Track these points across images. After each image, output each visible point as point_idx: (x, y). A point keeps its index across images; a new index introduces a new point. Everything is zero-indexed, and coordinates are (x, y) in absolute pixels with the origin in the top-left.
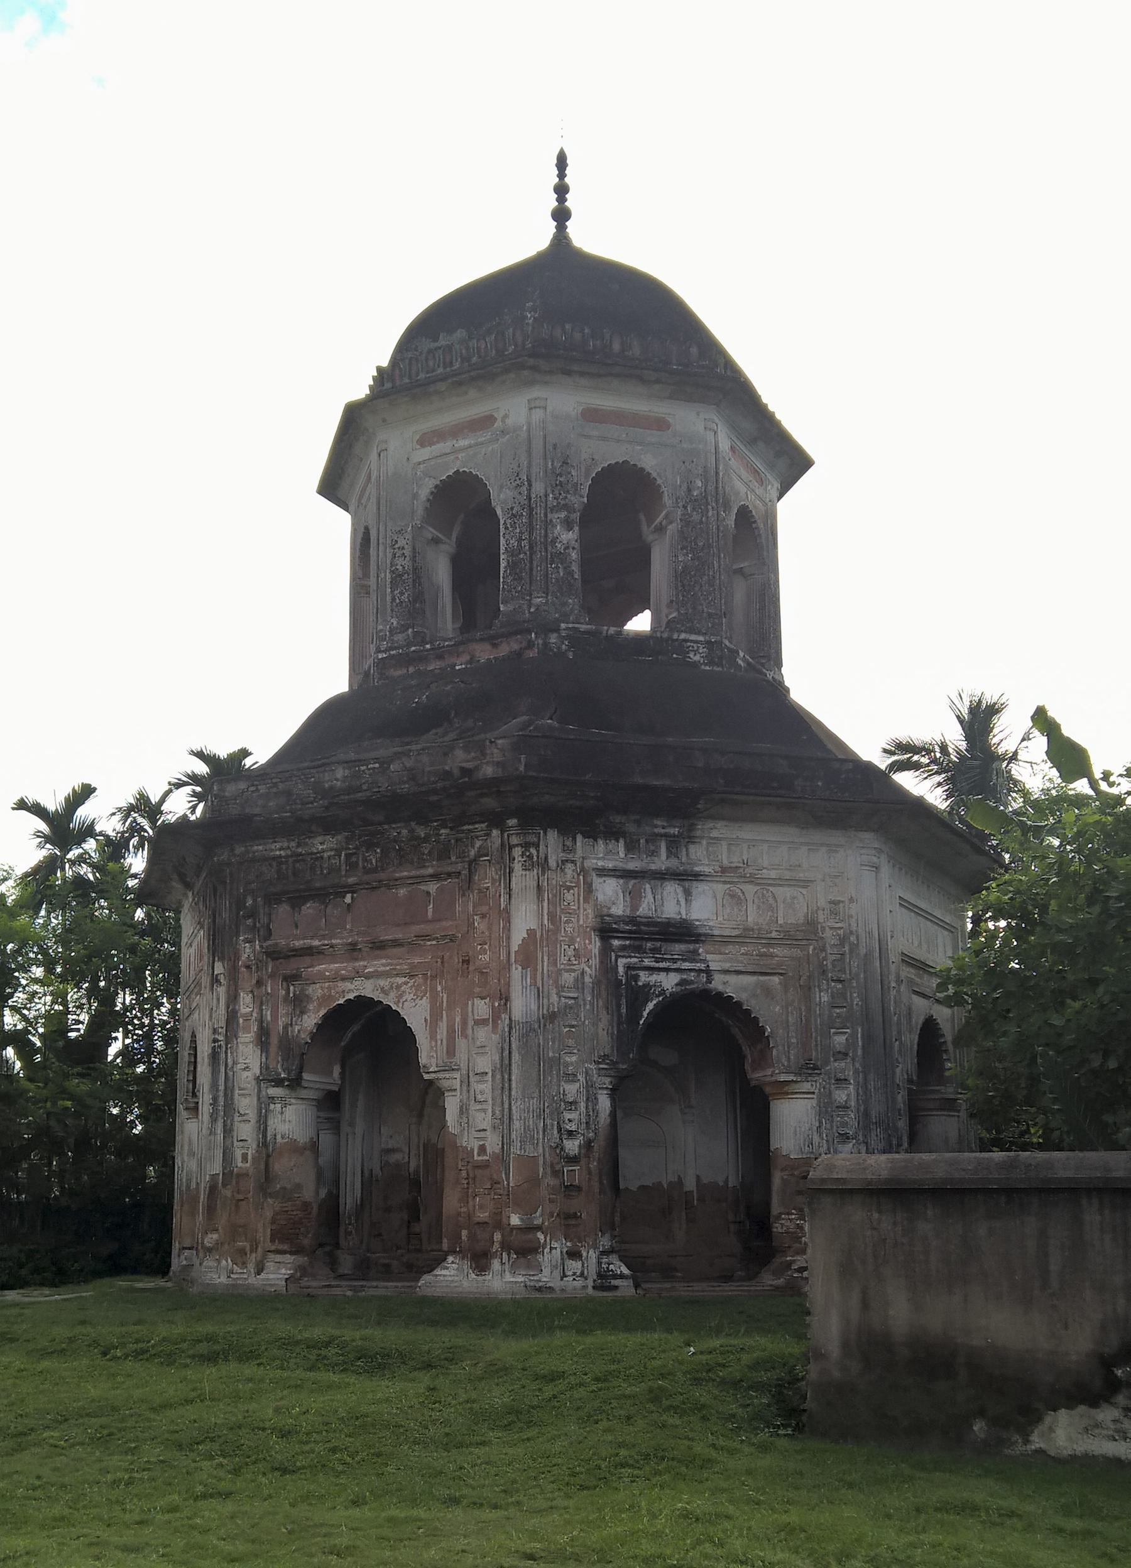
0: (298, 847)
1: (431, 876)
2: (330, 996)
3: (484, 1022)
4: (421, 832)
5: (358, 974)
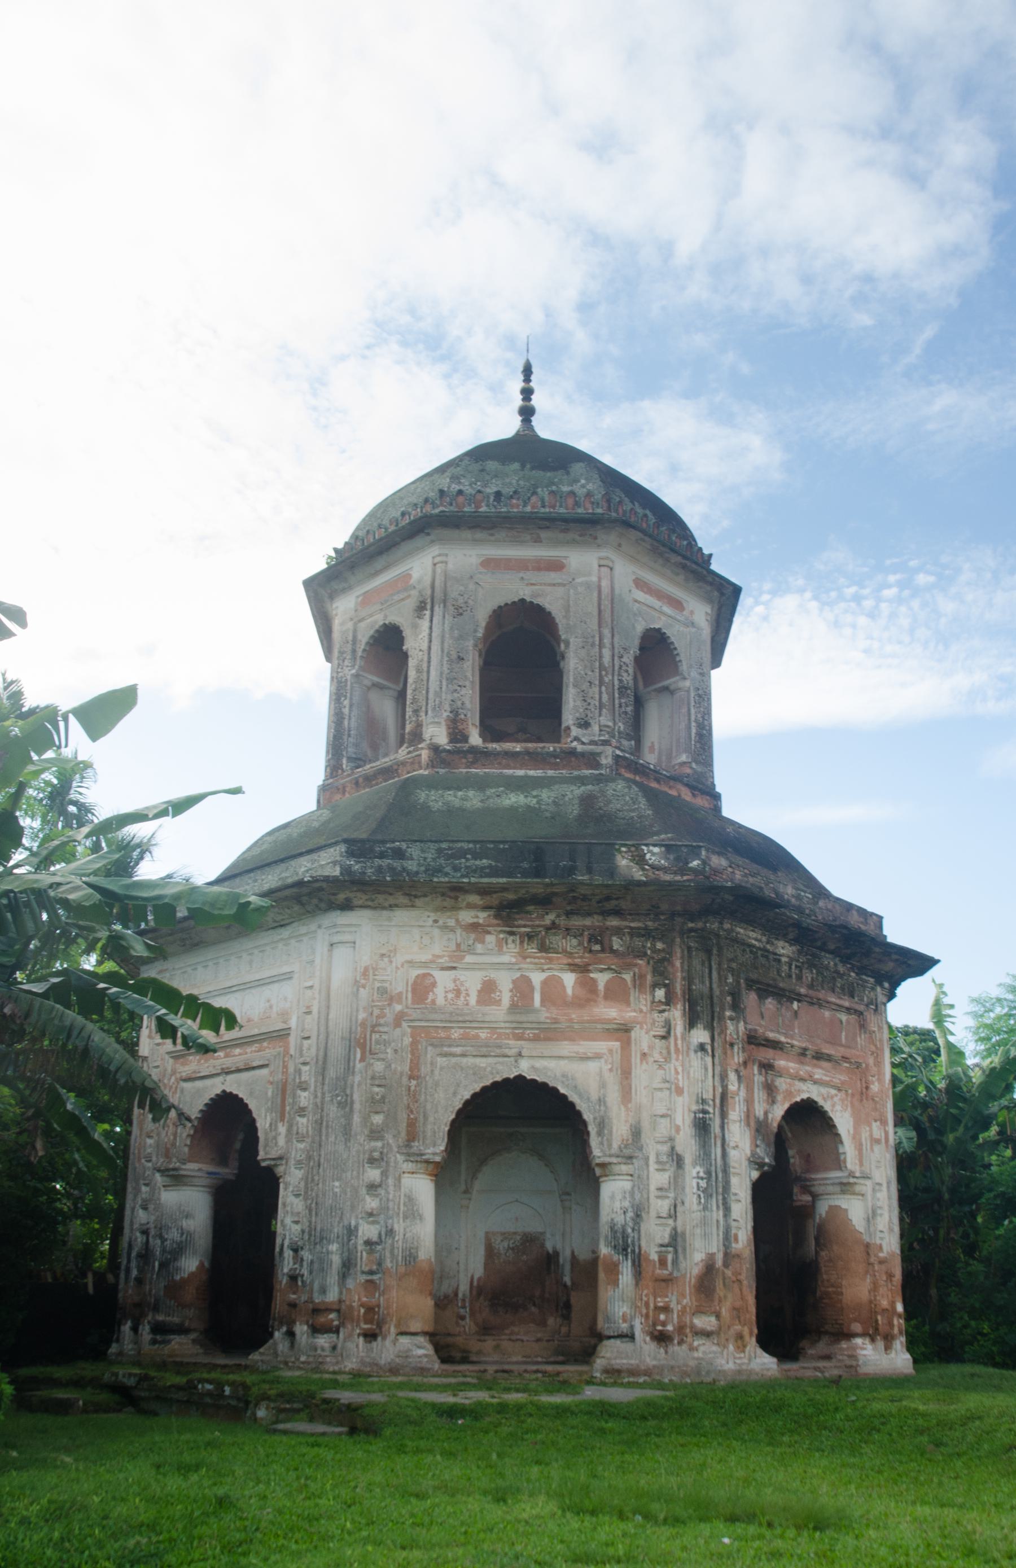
0: (768, 943)
1: (848, 1009)
2: (791, 1092)
3: (878, 1141)
4: (841, 969)
5: (810, 1079)
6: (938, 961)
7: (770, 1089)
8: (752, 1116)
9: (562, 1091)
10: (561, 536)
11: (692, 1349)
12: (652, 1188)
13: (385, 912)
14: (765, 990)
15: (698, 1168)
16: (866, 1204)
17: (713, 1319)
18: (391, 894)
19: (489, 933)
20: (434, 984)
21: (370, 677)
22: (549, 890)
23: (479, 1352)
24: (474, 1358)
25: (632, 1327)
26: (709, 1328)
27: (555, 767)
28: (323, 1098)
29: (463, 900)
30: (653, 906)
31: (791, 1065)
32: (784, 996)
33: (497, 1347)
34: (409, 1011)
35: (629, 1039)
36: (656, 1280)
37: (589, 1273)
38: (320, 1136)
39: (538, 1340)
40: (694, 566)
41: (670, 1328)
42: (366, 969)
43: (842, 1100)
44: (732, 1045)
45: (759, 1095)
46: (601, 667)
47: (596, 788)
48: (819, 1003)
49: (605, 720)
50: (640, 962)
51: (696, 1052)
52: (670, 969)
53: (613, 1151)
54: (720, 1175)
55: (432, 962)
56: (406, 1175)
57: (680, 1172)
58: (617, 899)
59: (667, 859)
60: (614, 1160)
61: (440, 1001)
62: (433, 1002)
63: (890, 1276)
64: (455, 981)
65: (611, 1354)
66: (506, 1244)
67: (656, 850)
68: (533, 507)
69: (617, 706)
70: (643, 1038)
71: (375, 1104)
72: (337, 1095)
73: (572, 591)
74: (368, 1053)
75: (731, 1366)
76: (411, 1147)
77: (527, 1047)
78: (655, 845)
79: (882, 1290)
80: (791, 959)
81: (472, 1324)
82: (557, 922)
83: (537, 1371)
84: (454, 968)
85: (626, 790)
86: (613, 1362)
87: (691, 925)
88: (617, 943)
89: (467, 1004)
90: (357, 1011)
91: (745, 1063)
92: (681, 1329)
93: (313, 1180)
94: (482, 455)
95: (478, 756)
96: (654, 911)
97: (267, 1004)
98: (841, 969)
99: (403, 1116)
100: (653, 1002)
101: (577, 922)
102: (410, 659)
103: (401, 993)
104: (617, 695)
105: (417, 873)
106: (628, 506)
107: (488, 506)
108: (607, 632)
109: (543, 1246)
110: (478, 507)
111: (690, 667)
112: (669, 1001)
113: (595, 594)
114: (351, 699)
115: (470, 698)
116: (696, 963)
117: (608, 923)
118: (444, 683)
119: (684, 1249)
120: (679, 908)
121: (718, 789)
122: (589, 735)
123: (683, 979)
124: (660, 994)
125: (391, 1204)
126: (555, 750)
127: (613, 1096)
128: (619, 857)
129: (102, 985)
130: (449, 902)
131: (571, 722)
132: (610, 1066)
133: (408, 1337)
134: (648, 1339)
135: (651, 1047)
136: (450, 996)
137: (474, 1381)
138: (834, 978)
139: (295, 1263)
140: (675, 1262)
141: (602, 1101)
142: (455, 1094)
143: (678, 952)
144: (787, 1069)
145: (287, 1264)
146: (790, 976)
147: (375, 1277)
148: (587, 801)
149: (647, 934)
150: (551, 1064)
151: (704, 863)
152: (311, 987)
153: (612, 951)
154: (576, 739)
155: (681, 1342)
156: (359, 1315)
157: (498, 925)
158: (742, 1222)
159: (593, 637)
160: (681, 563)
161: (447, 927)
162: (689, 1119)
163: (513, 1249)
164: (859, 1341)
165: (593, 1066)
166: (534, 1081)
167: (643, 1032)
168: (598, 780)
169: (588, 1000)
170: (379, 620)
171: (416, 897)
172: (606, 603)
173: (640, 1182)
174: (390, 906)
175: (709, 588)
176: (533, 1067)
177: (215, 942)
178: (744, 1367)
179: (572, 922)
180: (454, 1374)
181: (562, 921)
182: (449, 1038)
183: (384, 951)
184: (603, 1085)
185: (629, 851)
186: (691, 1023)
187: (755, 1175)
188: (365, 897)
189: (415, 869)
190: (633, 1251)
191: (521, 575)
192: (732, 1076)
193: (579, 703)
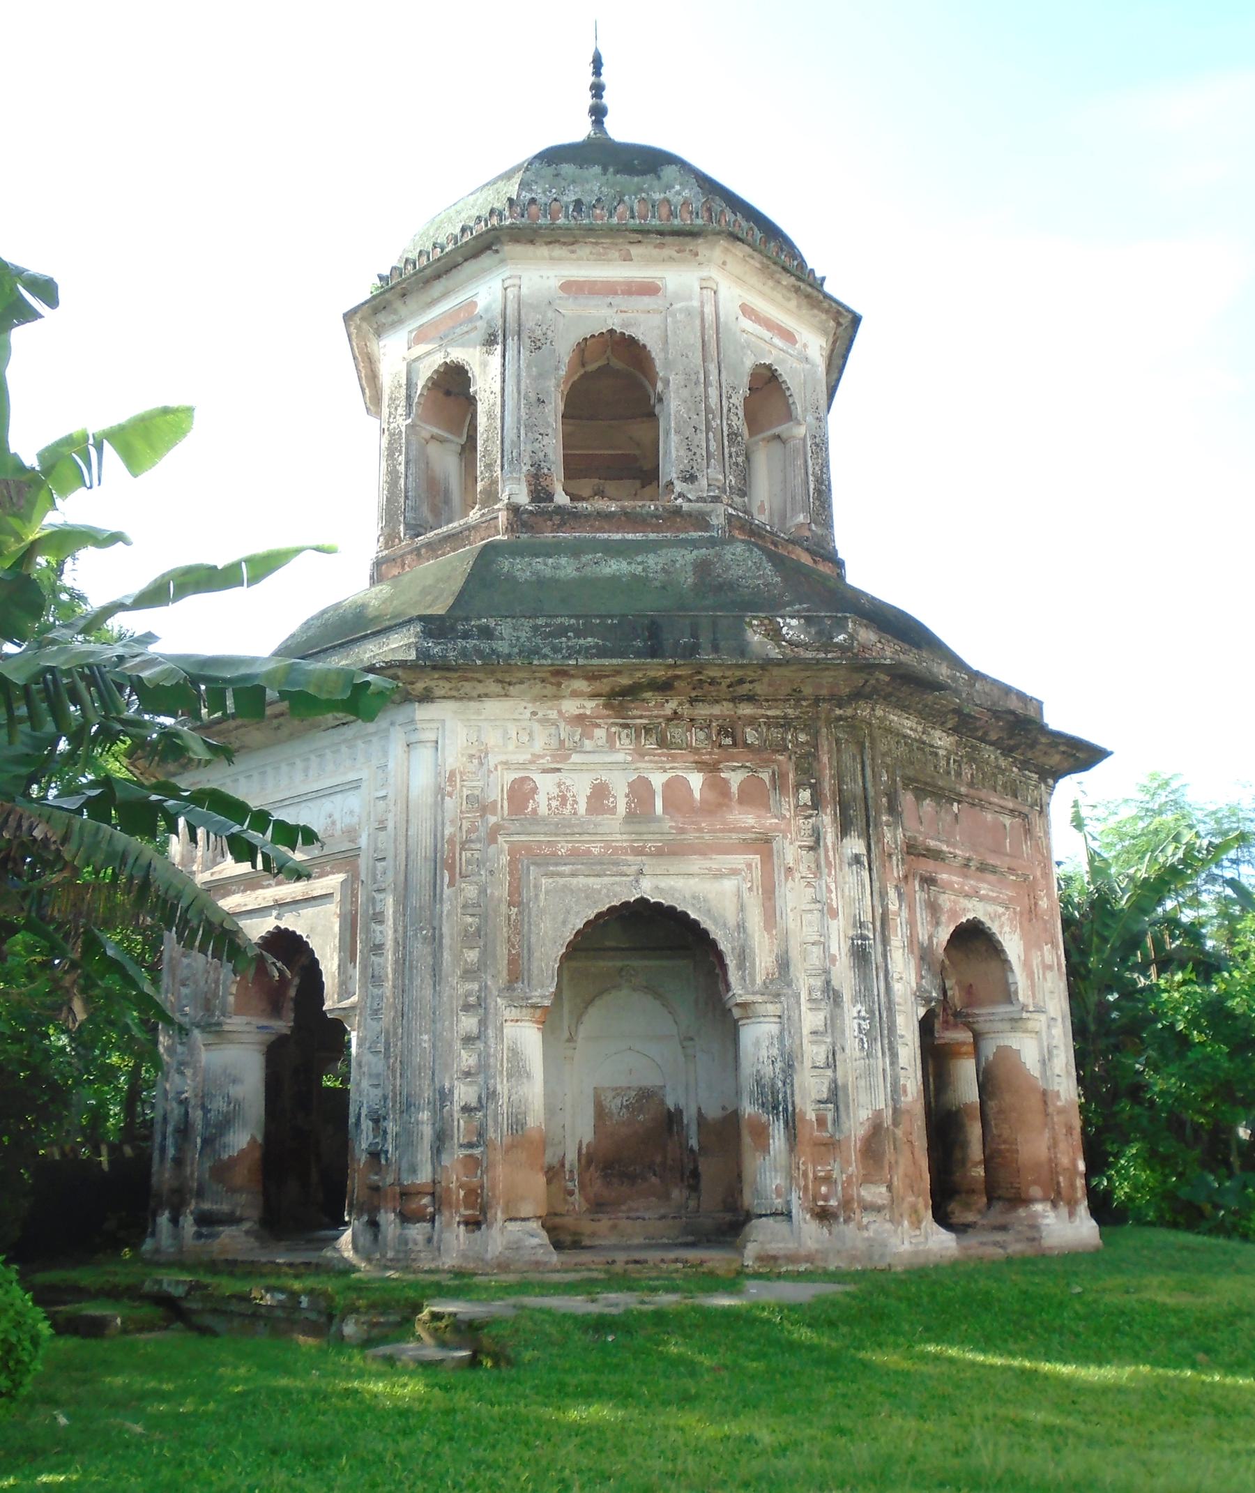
1: (1012, 811)
3: (1050, 968)
4: (1003, 763)
5: (974, 894)
6: (1110, 754)
7: (933, 908)
8: (915, 942)
9: (693, 916)
10: (655, 252)
11: (861, 1227)
12: (805, 1031)
13: (472, 704)
14: (922, 790)
15: (859, 1007)
16: (1040, 1041)
17: (883, 1189)
18: (480, 681)
19: (598, 726)
20: (535, 790)
21: (428, 427)
22: (670, 673)
23: (593, 1235)
24: (586, 1242)
25: (788, 1203)
26: (880, 1202)
27: (657, 528)
28: (405, 932)
29: (568, 687)
30: (795, 690)
31: (955, 878)
32: (942, 796)
33: (614, 1227)
34: (506, 824)
35: (771, 849)
36: (816, 1144)
37: (727, 1134)
38: (403, 978)
39: (663, 1217)
40: (809, 289)
41: (833, 1203)
42: (452, 774)
43: (1011, 920)
44: (890, 856)
45: (922, 915)
46: (708, 410)
47: (711, 551)
48: (978, 804)
49: (715, 473)
50: (781, 758)
51: (850, 865)
52: (815, 764)
53: (756, 988)
54: (885, 1015)
55: (530, 762)
56: (509, 1024)
57: (838, 1011)
58: (751, 682)
59: (808, 634)
60: (759, 998)
61: (543, 810)
62: (534, 811)
63: (1070, 1129)
64: (559, 785)
65: (764, 1238)
66: (618, 1101)
67: (794, 622)
68: (620, 218)
69: (727, 456)
70: (791, 851)
71: (471, 937)
72: (422, 929)
73: (669, 320)
74: (457, 876)
75: (906, 1247)
76: (514, 990)
77: (649, 864)
78: (792, 617)
79: (1063, 1146)
80: (949, 752)
81: (582, 1200)
82: (679, 711)
83: (676, 1261)
84: (559, 770)
85: (747, 554)
86: (768, 1246)
87: (838, 712)
88: (751, 736)
89: (575, 813)
90: (443, 824)
91: (906, 877)
92: (846, 1203)
93: (395, 1034)
94: (553, 157)
95: (566, 517)
96: (795, 696)
97: (329, 821)
98: (1003, 763)
99: (502, 952)
100: (797, 806)
101: (703, 711)
102: (479, 404)
103: (495, 801)
104: (726, 443)
105: (509, 656)
106: (729, 216)
107: (567, 217)
108: (713, 367)
109: (662, 1102)
110: (554, 218)
111: (805, 410)
112: (816, 804)
113: (698, 322)
114: (407, 453)
115: (553, 448)
116: (846, 757)
117: (740, 712)
118: (522, 432)
119: (847, 1107)
120: (824, 692)
121: (841, 555)
122: (696, 491)
123: (832, 777)
124: (805, 795)
125: (492, 1060)
126: (657, 509)
127: (755, 920)
128: (749, 632)
129: (154, 797)
130: (550, 690)
131: (674, 476)
132: (749, 885)
133: (519, 1223)
134: (808, 1217)
135: (797, 861)
136: (554, 803)
137: (602, 1276)
138: (994, 775)
139: (375, 1137)
140: (836, 1121)
141: (741, 927)
142: (564, 923)
143: (824, 745)
144: (951, 883)
145: (364, 1140)
146: (948, 773)
147: (476, 1152)
148: (702, 567)
149: (786, 724)
150: (679, 883)
151: (852, 637)
152: (384, 797)
153: (746, 745)
154: (681, 495)
155: (846, 1221)
156: (458, 1199)
157: (609, 717)
158: (911, 1070)
159: (697, 373)
160: (793, 286)
161: (548, 720)
162: (845, 946)
163: (627, 1107)
164: (1039, 1207)
165: (729, 885)
166: (659, 904)
167: (787, 842)
168: (712, 542)
169: (720, 805)
170: (437, 360)
171: (510, 684)
172: (711, 332)
173: (787, 1022)
174: (479, 696)
175: (824, 316)
176: (657, 887)
177: (265, 746)
178: (921, 1247)
179: (696, 712)
180: (576, 1268)
181: (685, 710)
182: (554, 854)
183: (473, 752)
184: (742, 908)
185: (762, 624)
186: (844, 829)
187: (922, 1012)
188: (448, 685)
189: (506, 651)
190: (786, 1110)
191: (609, 300)
192: (892, 894)
193: (682, 453)
